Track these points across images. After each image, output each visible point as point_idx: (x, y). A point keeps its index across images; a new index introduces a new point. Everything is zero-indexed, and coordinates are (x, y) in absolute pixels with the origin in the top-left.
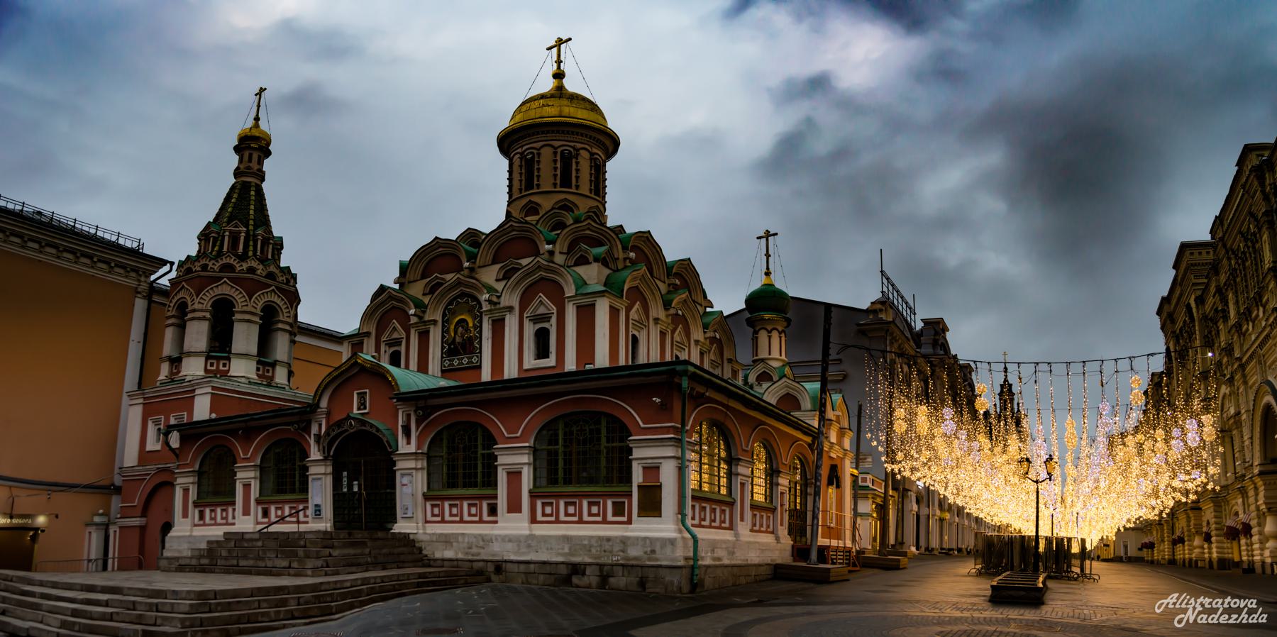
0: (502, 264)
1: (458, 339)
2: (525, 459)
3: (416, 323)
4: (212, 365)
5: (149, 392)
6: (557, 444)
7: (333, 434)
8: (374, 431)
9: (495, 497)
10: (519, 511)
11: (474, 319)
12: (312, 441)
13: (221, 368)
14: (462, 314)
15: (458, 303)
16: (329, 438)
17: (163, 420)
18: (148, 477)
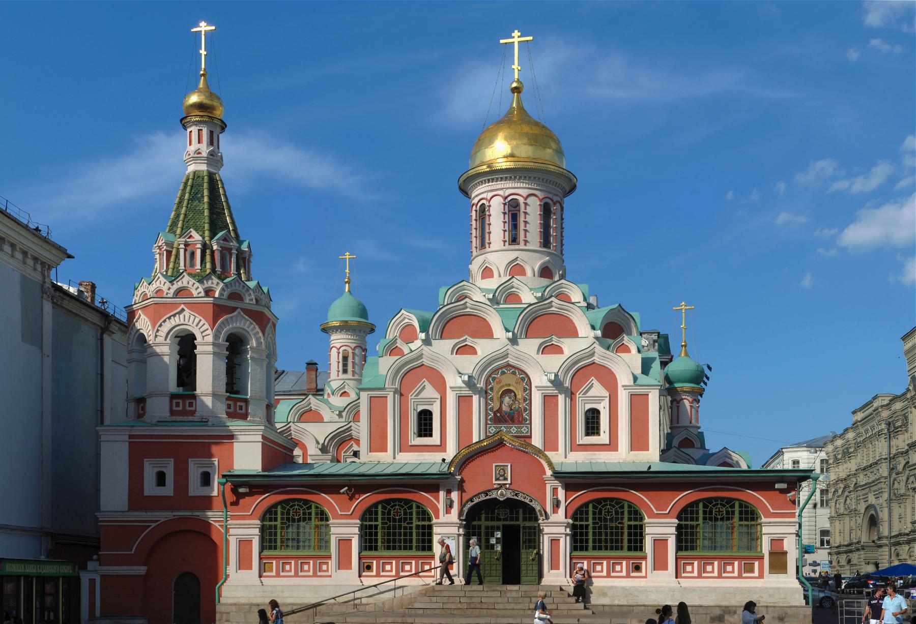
0: (543, 340)
1: (505, 408)
2: (673, 530)
3: (460, 387)
4: (229, 406)
5: (140, 430)
6: (697, 520)
7: (476, 501)
8: (527, 501)
9: (645, 558)
10: (667, 569)
11: (525, 390)
12: (441, 506)
13: (239, 411)
14: (509, 385)
15: (503, 373)
16: (472, 504)
17: (173, 462)
18: (154, 525)
